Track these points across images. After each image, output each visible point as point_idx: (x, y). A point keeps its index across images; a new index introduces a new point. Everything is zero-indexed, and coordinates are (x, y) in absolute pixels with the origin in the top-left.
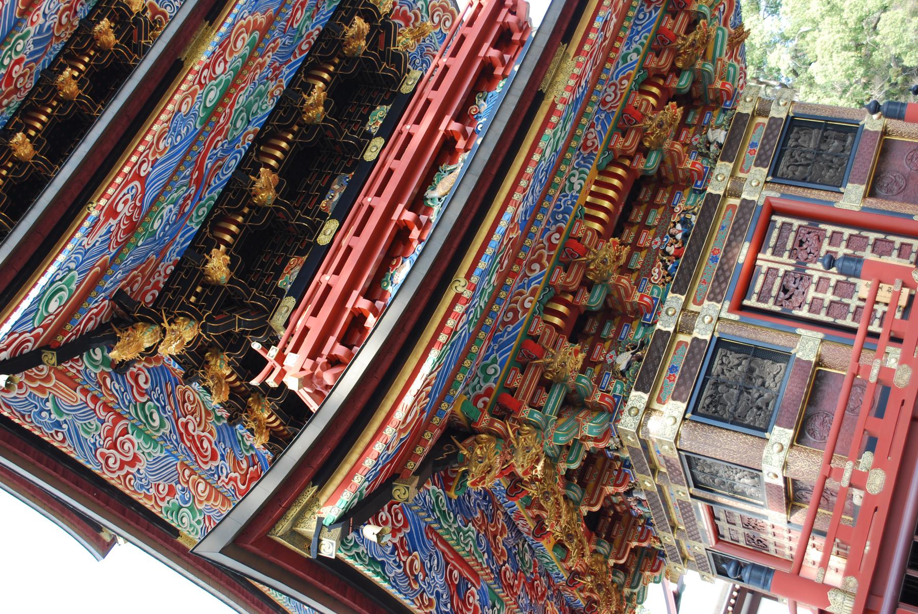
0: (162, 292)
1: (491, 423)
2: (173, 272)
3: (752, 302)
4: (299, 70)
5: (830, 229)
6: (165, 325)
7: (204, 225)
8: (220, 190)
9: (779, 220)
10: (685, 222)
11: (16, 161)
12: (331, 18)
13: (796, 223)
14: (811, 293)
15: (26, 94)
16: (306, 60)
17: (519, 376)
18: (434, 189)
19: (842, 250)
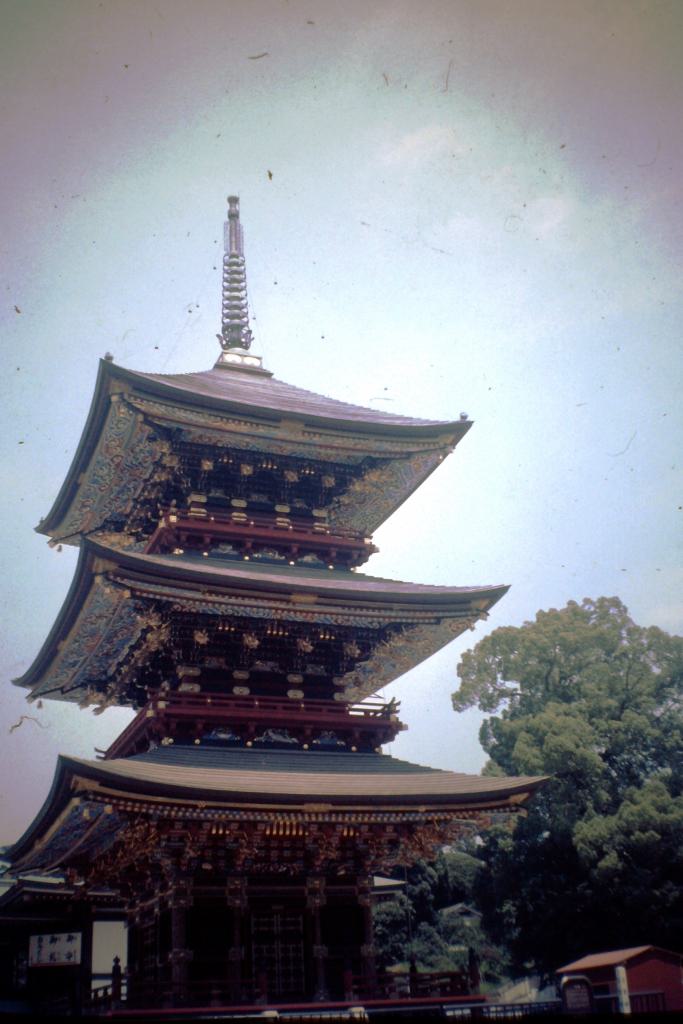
0: (181, 612)
1: (153, 827)
2: (193, 613)
3: (253, 920)
4: (324, 624)
5: (302, 945)
6: (164, 626)
7: (223, 616)
8: (244, 615)
9: (301, 919)
10: (288, 870)
11: (239, 465)
12: (361, 628)
13: (301, 928)
14: (264, 947)
15: (280, 453)
16: (331, 625)
17: (180, 827)
18: (274, 732)
19: (291, 955)
